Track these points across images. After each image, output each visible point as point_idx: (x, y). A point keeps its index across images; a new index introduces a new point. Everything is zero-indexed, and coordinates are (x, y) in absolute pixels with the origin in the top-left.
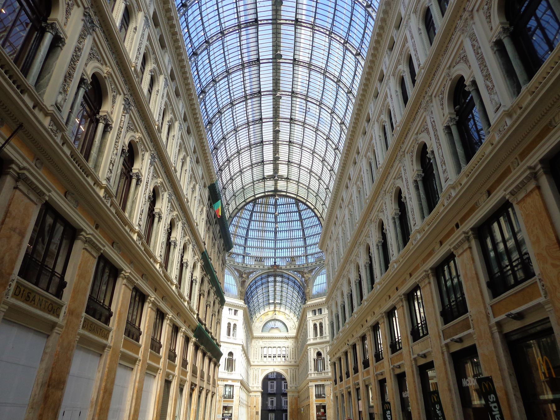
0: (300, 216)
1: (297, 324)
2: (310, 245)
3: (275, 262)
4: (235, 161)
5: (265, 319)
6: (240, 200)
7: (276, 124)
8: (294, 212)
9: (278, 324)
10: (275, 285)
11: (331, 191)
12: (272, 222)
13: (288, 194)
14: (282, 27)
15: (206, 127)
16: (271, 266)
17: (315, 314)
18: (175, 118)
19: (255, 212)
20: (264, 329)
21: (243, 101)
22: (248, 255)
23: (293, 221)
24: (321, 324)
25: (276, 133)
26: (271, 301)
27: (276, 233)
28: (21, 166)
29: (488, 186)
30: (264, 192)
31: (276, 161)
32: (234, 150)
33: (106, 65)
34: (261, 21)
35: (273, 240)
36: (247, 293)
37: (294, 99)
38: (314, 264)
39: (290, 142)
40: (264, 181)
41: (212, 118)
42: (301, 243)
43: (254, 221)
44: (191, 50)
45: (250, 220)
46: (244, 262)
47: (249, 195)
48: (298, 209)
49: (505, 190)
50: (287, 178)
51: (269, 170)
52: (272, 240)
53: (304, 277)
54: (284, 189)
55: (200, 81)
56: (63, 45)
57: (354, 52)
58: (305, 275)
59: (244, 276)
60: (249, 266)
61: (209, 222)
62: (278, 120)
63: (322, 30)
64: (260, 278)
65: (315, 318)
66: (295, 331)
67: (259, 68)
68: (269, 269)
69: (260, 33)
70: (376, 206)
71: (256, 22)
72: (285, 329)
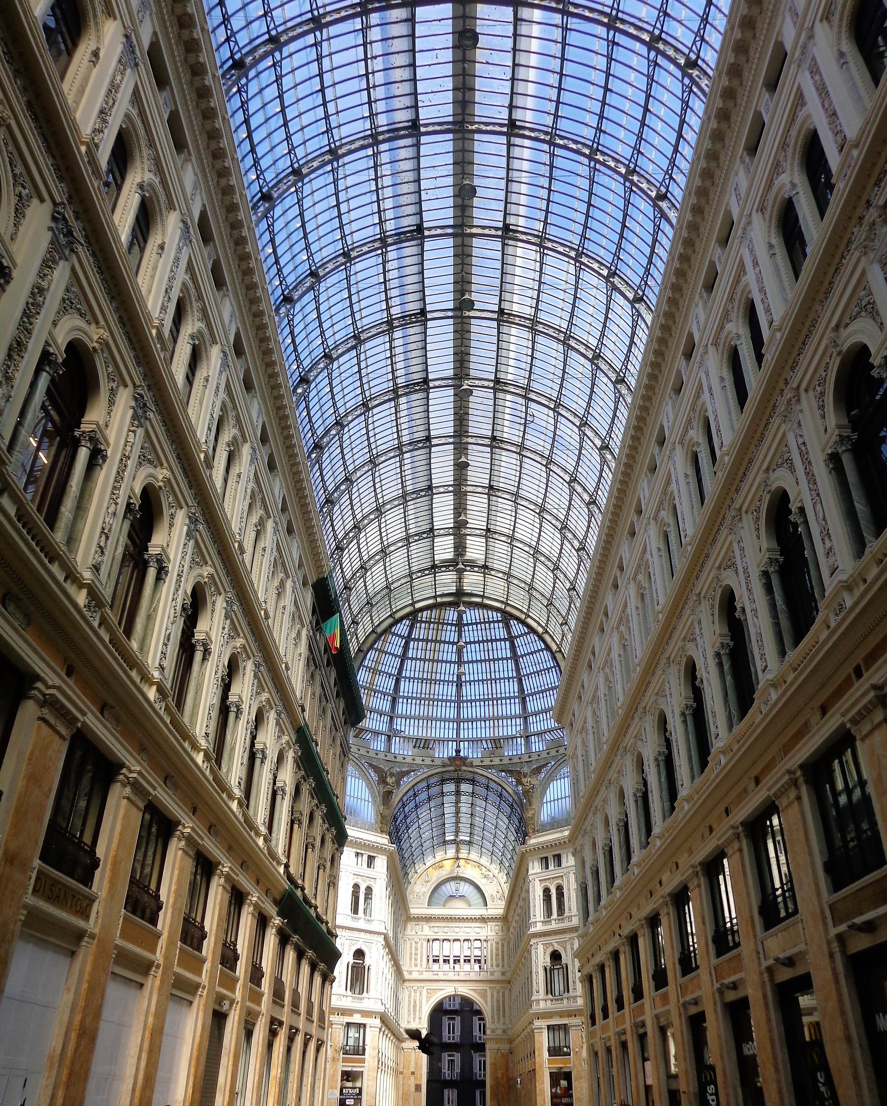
0: (513, 648)
1: (506, 888)
2: (536, 714)
3: (458, 751)
4: (378, 569)
6: (381, 614)
7: (461, 449)
8: (500, 640)
10: (458, 802)
11: (573, 628)
12: (451, 662)
13: (486, 601)
14: (476, 242)
15: (309, 456)
16: (450, 759)
17: (547, 868)
18: (267, 513)
19: (414, 640)
21: (389, 400)
22: (397, 733)
23: (498, 659)
25: (461, 468)
26: (449, 837)
27: (459, 686)
28: (50, 683)
29: (754, 772)
30: (435, 597)
31: (459, 529)
32: (375, 547)
33: (97, 323)
34: (430, 229)
35: (454, 701)
36: (395, 819)
37: (500, 395)
38: (544, 755)
39: (491, 487)
40: (435, 573)
41: (323, 437)
42: (517, 709)
43: (412, 659)
44: (279, 291)
45: (404, 657)
46: (389, 751)
47: (402, 602)
48: (509, 633)
49: (843, 715)
50: (485, 567)
51: (444, 549)
52: (451, 701)
53: (522, 784)
54: (478, 590)
55: (312, 427)
56: (104, 461)
57: (631, 296)
58: (524, 780)
59: (390, 780)
60: (400, 759)
61: (312, 661)
62: (465, 440)
63: (561, 249)
64: (425, 784)
66: (502, 904)
67: (426, 329)
68: (444, 766)
69: (426, 255)
70: (653, 685)
71: (418, 233)
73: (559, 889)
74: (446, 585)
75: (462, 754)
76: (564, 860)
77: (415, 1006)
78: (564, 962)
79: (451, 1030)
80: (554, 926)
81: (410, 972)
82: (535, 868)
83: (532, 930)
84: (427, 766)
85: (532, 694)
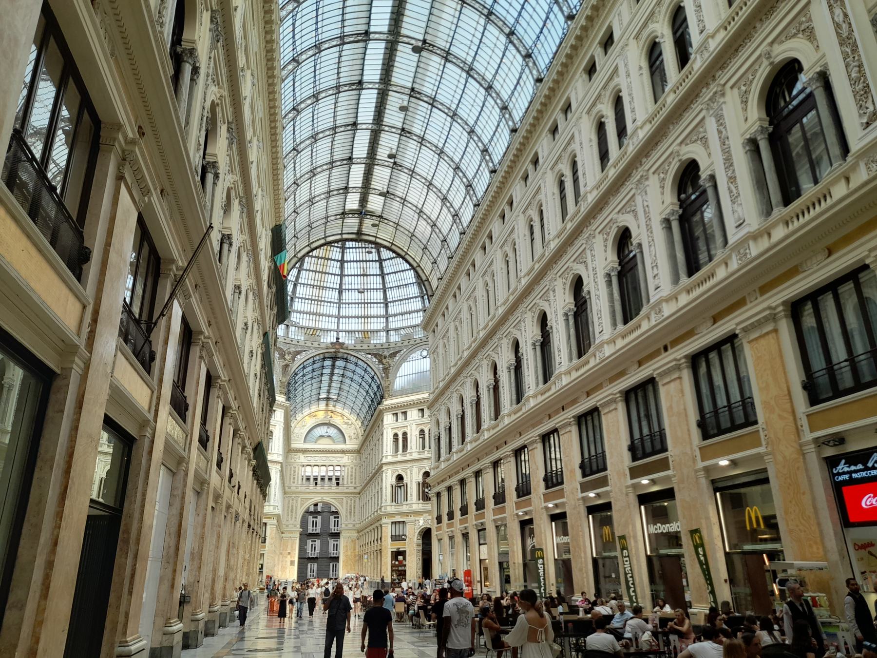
0: (381, 267)
1: (361, 432)
2: (395, 315)
3: (338, 339)
5: (310, 422)
9: (332, 431)
12: (335, 275)
13: (378, 240)
16: (332, 343)
20: (308, 438)
24: (405, 434)
27: (340, 292)
30: (341, 234)
42: (382, 311)
43: (306, 270)
48: (379, 256)
50: (381, 217)
51: (353, 201)
52: (334, 303)
58: (384, 361)
65: (396, 425)
72: (342, 439)
73: (405, 434)
74: (350, 226)
75: (340, 341)
76: (409, 414)
77: (292, 509)
78: (405, 482)
79: (314, 524)
80: (400, 458)
81: (290, 487)
82: (388, 418)
83: (384, 461)
84: (315, 348)
85: (393, 302)
